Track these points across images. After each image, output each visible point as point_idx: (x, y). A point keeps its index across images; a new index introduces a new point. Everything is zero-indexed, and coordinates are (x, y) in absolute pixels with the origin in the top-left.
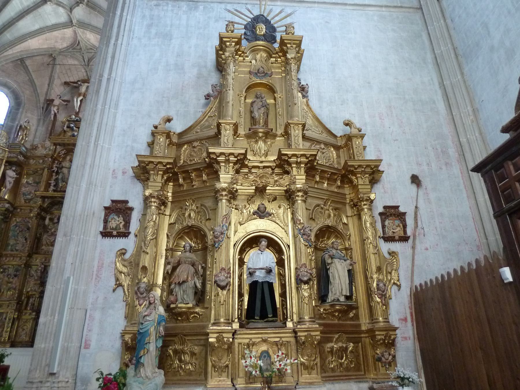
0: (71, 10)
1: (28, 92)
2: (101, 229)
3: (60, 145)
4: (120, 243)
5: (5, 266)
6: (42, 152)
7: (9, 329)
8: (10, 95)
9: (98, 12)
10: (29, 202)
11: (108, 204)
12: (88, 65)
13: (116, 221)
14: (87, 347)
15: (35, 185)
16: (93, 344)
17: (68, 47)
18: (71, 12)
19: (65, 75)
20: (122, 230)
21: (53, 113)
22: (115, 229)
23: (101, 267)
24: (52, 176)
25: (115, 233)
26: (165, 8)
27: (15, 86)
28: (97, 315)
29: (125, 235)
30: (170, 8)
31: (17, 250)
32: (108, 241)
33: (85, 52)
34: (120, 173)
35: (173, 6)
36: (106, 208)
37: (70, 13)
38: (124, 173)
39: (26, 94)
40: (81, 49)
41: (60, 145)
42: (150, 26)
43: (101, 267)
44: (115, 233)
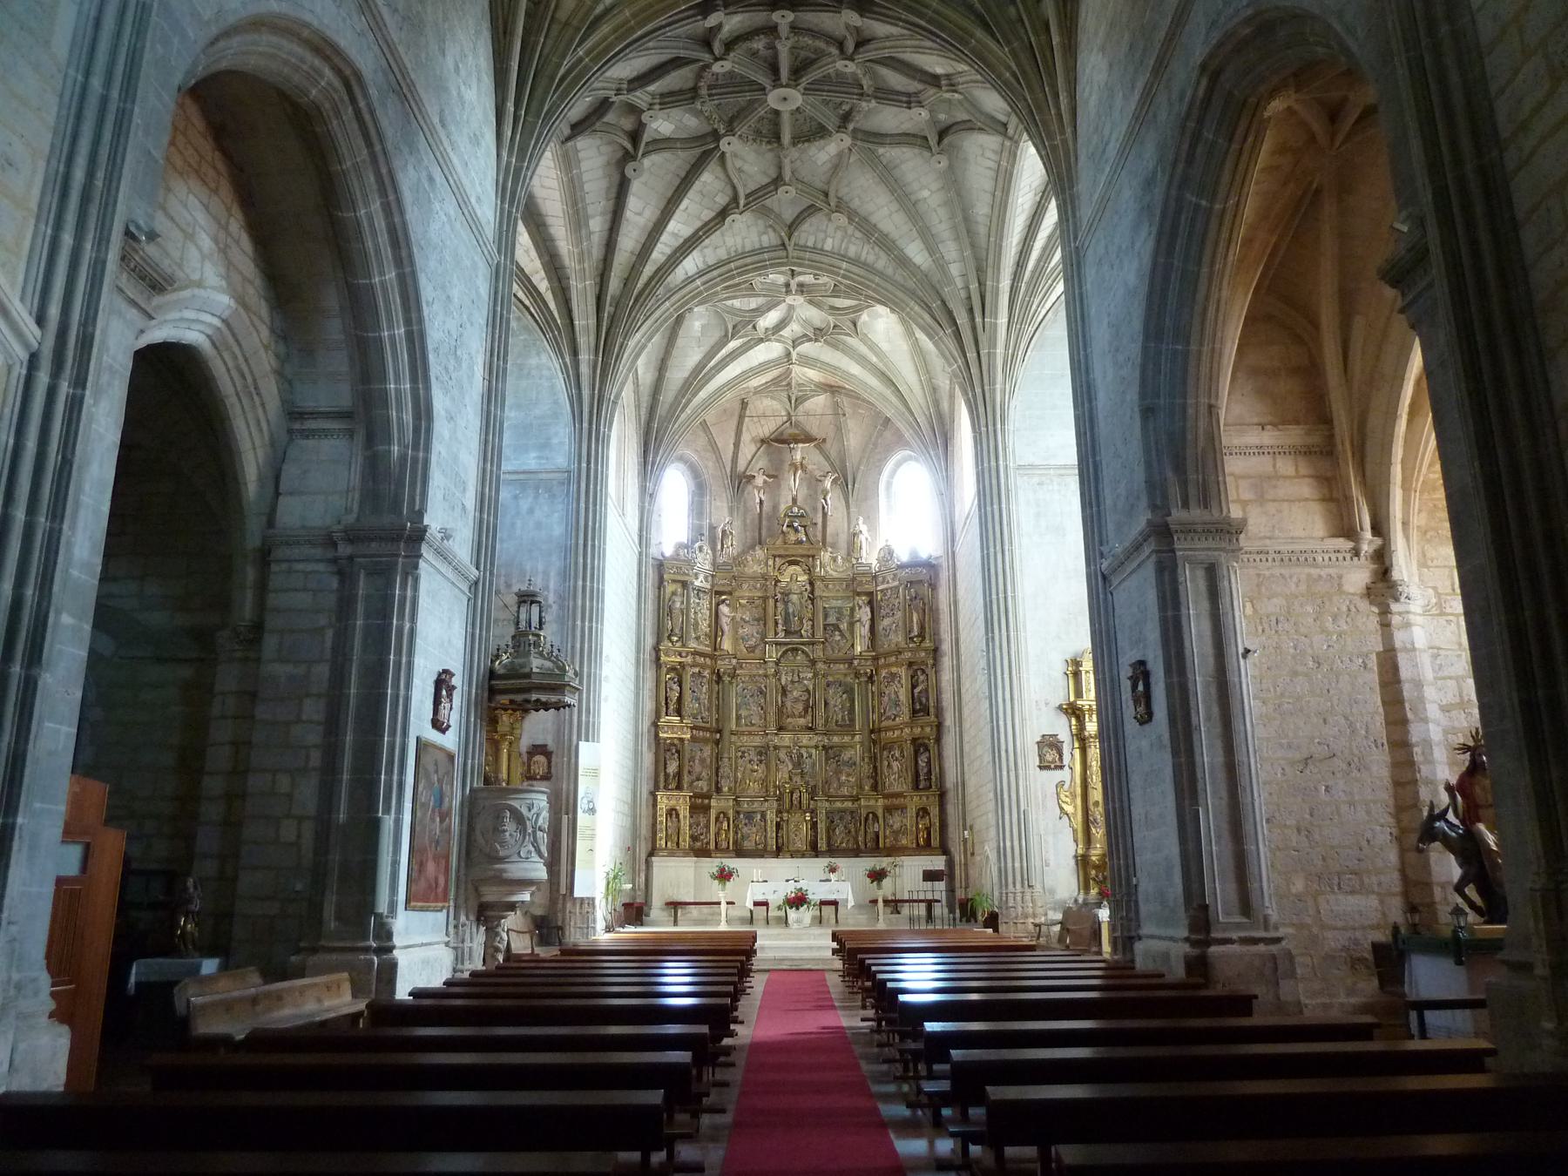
0: (795, 343)
1: (710, 464)
2: (1038, 763)
3: (779, 556)
4: (1058, 775)
5: (743, 749)
6: (755, 568)
7: (774, 835)
8: (688, 473)
9: (843, 351)
10: (753, 652)
11: (1039, 739)
12: (796, 407)
13: (1051, 756)
14: (1047, 865)
15: (756, 623)
16: (1052, 863)
17: (767, 383)
18: (794, 347)
19: (758, 425)
20: (1058, 764)
21: (758, 501)
22: (1052, 762)
23: (1045, 797)
24: (776, 607)
25: (1053, 766)
26: (1050, 488)
27: (694, 457)
28: (1050, 839)
29: (1061, 767)
30: (1056, 487)
31: (753, 725)
32: (1045, 773)
33: (795, 392)
34: (1042, 706)
35: (1059, 484)
36: (1038, 743)
37: (791, 349)
38: (1047, 704)
39: (709, 468)
40: (789, 384)
41: (779, 556)
42: (1038, 515)
43: (1045, 797)
44: (1053, 766)
